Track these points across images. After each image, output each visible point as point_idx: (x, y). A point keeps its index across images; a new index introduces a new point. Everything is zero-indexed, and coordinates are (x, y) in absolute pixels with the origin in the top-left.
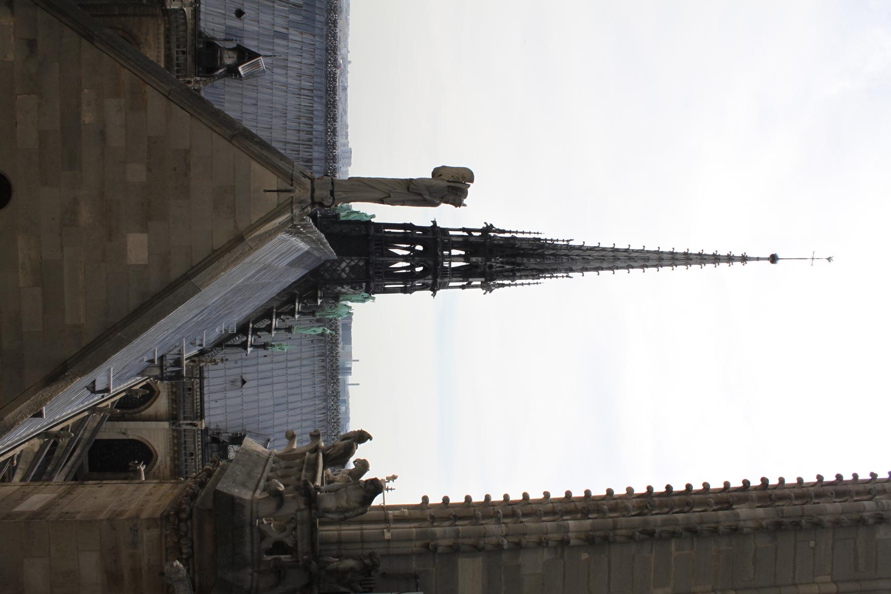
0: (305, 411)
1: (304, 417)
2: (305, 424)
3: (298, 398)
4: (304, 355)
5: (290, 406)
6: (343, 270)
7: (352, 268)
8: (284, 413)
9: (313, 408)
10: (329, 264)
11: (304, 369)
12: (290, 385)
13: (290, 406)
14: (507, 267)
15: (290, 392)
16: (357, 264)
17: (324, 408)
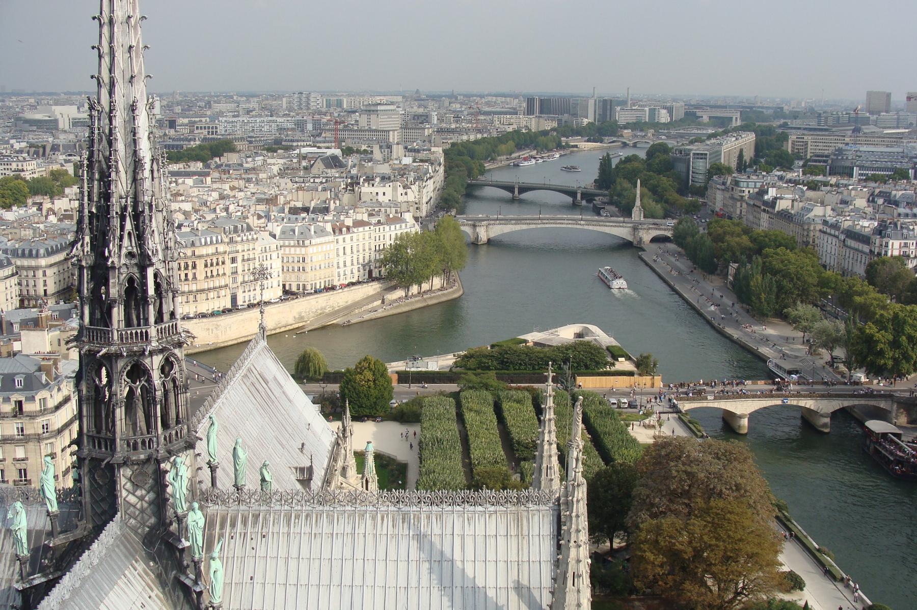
0: (370, 555)
1: (381, 555)
2: (392, 555)
3: (348, 565)
4: (282, 553)
5: (358, 581)
6: (141, 498)
7: (136, 486)
8: (368, 592)
9: (370, 539)
10: (132, 521)
11: (305, 553)
12: (325, 580)
13: (358, 581)
14: (128, 226)
15: (336, 581)
16: (130, 479)
17: (374, 518)
